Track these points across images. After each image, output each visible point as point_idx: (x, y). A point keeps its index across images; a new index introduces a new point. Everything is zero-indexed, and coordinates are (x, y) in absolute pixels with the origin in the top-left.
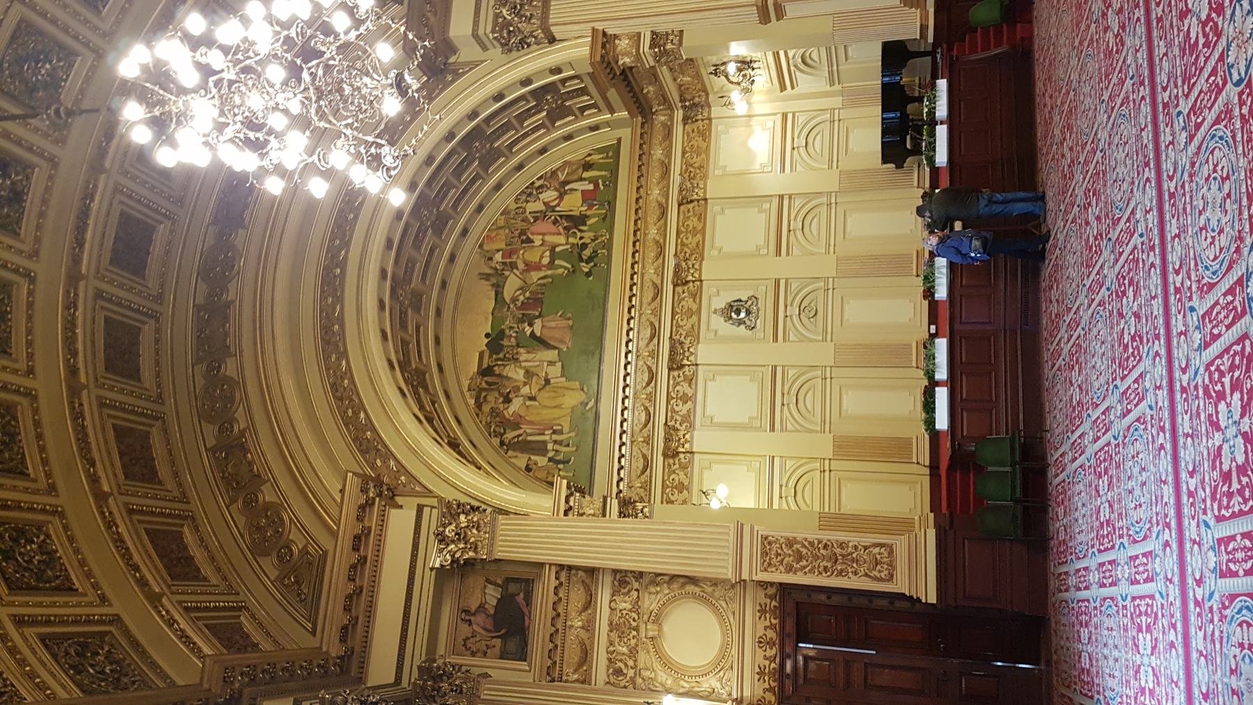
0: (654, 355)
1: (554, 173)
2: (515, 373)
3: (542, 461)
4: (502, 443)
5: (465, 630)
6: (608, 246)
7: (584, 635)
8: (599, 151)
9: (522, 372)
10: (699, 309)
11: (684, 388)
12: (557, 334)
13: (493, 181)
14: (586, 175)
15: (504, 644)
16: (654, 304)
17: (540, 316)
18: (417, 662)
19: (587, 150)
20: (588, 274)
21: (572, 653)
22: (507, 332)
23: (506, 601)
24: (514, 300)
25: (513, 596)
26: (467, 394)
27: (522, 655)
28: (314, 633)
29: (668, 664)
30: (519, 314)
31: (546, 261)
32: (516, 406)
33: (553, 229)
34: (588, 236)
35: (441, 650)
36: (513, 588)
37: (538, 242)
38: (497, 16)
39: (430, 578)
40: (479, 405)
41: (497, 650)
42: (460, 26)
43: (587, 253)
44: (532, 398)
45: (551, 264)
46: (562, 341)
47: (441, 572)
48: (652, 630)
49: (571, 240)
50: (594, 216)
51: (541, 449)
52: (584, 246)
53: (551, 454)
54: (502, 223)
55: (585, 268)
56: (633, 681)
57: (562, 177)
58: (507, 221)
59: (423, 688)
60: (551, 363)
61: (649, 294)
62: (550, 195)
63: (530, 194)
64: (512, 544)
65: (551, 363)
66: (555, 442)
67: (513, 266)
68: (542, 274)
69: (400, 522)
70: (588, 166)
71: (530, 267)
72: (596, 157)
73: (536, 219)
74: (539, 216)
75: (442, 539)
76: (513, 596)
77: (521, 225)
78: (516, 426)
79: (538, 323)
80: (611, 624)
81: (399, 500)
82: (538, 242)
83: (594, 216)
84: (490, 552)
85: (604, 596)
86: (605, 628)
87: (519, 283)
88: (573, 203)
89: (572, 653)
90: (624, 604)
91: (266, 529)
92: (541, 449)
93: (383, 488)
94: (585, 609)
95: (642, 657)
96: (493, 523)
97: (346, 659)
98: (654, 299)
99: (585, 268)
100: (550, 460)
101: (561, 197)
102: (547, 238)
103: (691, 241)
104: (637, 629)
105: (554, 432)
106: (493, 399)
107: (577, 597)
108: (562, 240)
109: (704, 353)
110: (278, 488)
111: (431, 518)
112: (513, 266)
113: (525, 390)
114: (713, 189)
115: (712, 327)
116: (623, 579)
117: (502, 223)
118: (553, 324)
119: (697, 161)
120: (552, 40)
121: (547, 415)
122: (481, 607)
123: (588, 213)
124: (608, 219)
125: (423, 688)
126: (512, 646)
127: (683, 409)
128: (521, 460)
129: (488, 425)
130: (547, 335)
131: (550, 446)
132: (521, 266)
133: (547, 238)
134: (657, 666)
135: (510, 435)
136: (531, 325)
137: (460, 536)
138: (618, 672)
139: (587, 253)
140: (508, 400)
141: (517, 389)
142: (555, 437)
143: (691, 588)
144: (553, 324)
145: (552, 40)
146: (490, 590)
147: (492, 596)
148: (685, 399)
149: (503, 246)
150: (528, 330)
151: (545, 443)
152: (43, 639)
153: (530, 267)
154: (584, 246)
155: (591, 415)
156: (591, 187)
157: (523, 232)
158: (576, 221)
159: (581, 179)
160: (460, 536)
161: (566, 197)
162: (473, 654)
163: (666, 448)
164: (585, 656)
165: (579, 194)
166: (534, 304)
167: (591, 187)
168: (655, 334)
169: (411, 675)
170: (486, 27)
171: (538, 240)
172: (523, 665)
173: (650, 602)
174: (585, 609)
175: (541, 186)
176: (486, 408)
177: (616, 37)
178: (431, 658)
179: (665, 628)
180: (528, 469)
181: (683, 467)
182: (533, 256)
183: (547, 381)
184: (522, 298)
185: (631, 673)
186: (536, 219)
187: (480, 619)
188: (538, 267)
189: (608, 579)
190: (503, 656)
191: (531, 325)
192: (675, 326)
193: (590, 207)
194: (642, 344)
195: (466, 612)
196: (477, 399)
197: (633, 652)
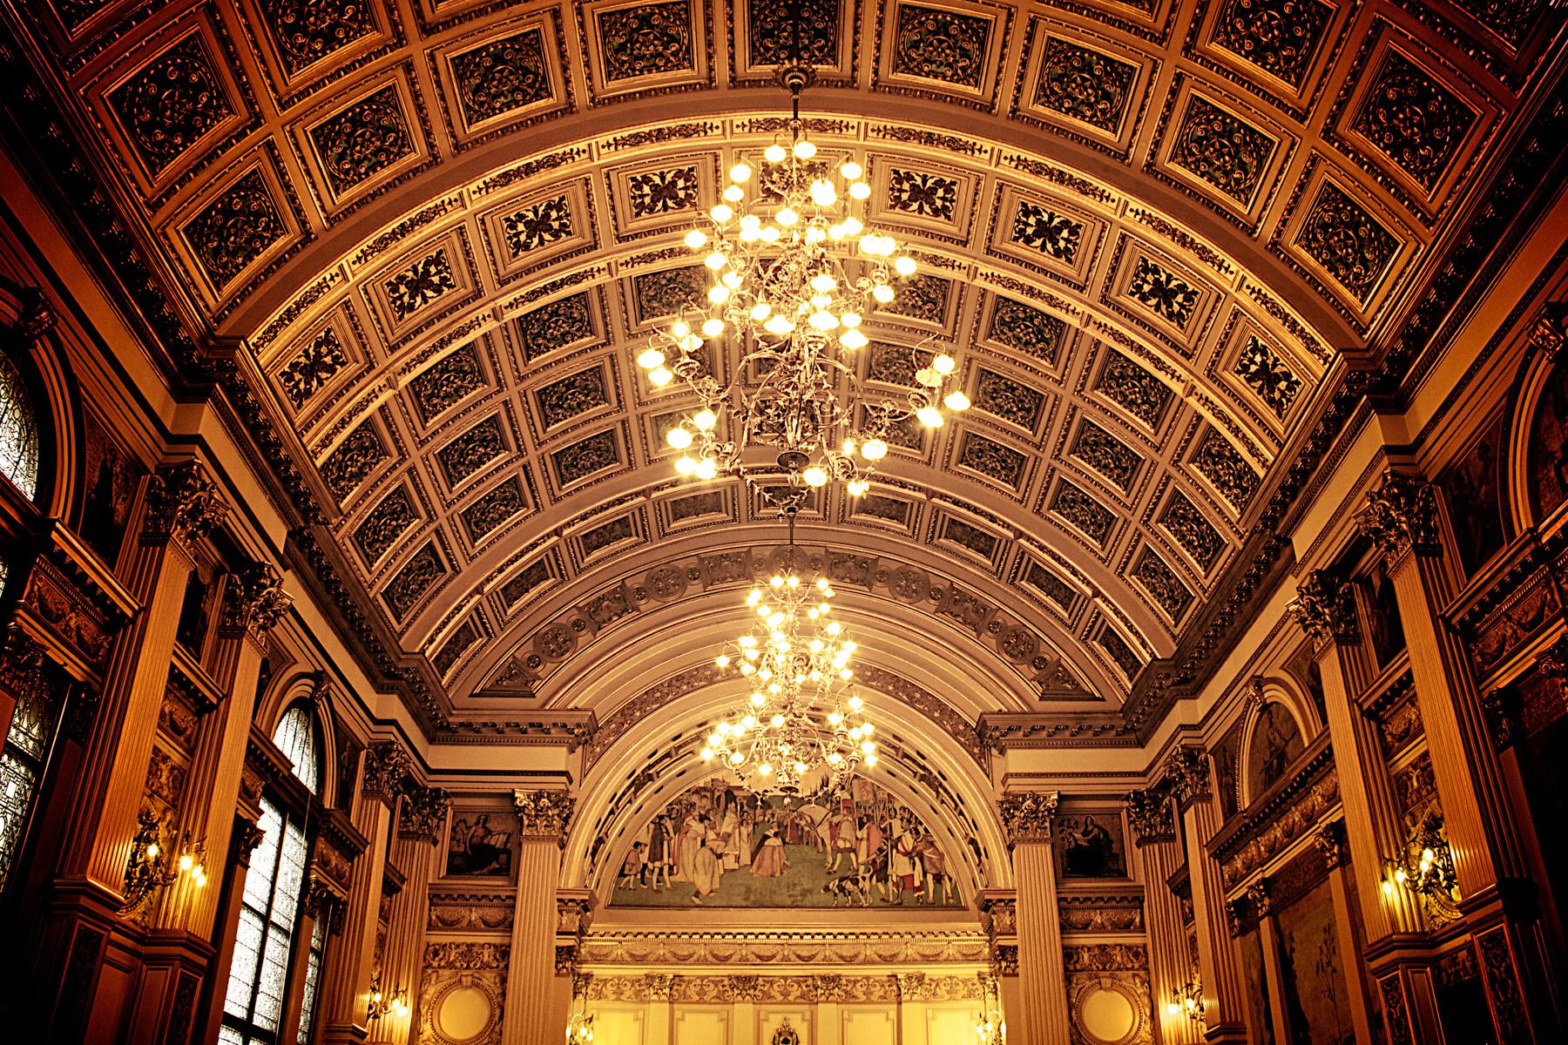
0: (744, 961)
1: (932, 844)
2: (728, 824)
3: (644, 858)
4: (661, 817)
5: (472, 820)
6: (856, 906)
7: (465, 923)
8: (954, 889)
9: (729, 830)
10: (790, 1003)
11: (712, 991)
12: (767, 862)
13: (916, 784)
14: (930, 877)
15: (461, 854)
16: (793, 957)
17: (784, 842)
18: (442, 786)
19: (954, 877)
20: (827, 889)
21: (450, 913)
22: (769, 812)
23: (493, 852)
24: (801, 816)
25: (497, 860)
26: (709, 779)
27: (453, 870)
28: (472, 695)
29: (441, 995)
30: (787, 822)
31: (841, 844)
32: (697, 827)
33: (874, 849)
34: (866, 885)
35: (458, 801)
36: (503, 857)
37: (859, 834)
38: (1024, 796)
39: (506, 788)
40: (697, 791)
41: (455, 849)
42: (1019, 760)
43: (848, 885)
44: (703, 843)
45: (836, 850)
46: (759, 867)
47: (511, 796)
48: (467, 981)
49: (862, 868)
50: (887, 890)
51: (655, 856)
52: (856, 882)
53: (650, 866)
54: (880, 795)
55: (833, 885)
56: (430, 966)
57: (926, 853)
58: (882, 801)
59: (425, 795)
60: (738, 859)
61: (805, 953)
62: (908, 842)
63: (909, 822)
64: (535, 860)
65: (738, 859)
66: (661, 869)
67: (835, 812)
68: (827, 842)
69: (555, 757)
70: (938, 879)
71: (835, 828)
72: (948, 886)
73: (884, 830)
74: (886, 832)
75: (538, 796)
76: (497, 860)
77: (878, 814)
78: (677, 830)
79: (778, 842)
80: (472, 945)
81: (579, 750)
82: (859, 834)
83: (887, 890)
84: (531, 839)
85: (493, 938)
86: (470, 940)
87: (818, 819)
88: (900, 866)
89: (450, 913)
90: (486, 956)
91: (555, 643)
92: (655, 856)
93: (587, 736)
94: (485, 922)
95: (447, 972)
96: (550, 838)
97: (448, 728)
98: (799, 956)
99: (833, 885)
100: (645, 866)
101: (906, 854)
102: (864, 844)
103: (859, 991)
104: (468, 967)
105: (671, 868)
106: (703, 804)
107: (494, 914)
108: (863, 858)
109: (743, 1011)
110: (588, 646)
111: (558, 784)
112: (835, 812)
113: (711, 835)
114: (913, 1011)
115: (772, 1017)
116: (504, 952)
117: (880, 795)
118: (776, 856)
119: (942, 991)
120: (1010, 848)
121: (687, 859)
122: (489, 832)
123: (890, 883)
124: (886, 905)
125: (425, 795)
126: (458, 861)
127: (692, 991)
128: (645, 837)
129: (679, 802)
130: (768, 851)
131: (658, 864)
132: (836, 820)
133: (864, 844)
134: (441, 986)
135: (669, 824)
136: (776, 835)
137: (539, 812)
138: (436, 953)
139: (848, 885)
140: (702, 819)
141: (713, 828)
142: (666, 869)
143: (498, 1012)
144: (776, 856)
145: (1010, 848)
146: (503, 838)
147: (497, 841)
148: (702, 993)
149: (857, 798)
150: (770, 833)
151: (662, 858)
152: (430, 545)
153: (835, 828)
154: (856, 882)
155: (686, 902)
156: (917, 884)
157: (870, 818)
158: (880, 871)
159: (925, 874)
160: (539, 812)
161: (906, 859)
162: (453, 829)
163: (653, 977)
164: (449, 925)
165: (909, 871)
166: (796, 835)
167: (917, 884)
168: (765, 959)
169: (432, 783)
170: (1016, 787)
171: (862, 834)
172: (443, 873)
173: (489, 979)
174: (485, 922)
175: (918, 833)
176: (695, 798)
177: (1013, 912)
178: (447, 795)
179: (470, 992)
180: (637, 845)
181: (637, 994)
182: (846, 830)
183: (719, 856)
184: (803, 823)
185: (435, 964)
186: (884, 830)
187: (481, 832)
188: (833, 838)
189: (506, 941)
190: (451, 854)
191: (776, 835)
192: (770, 981)
193: (896, 885)
194: (754, 948)
195: (485, 821)
196: (705, 789)
197: (450, 965)
